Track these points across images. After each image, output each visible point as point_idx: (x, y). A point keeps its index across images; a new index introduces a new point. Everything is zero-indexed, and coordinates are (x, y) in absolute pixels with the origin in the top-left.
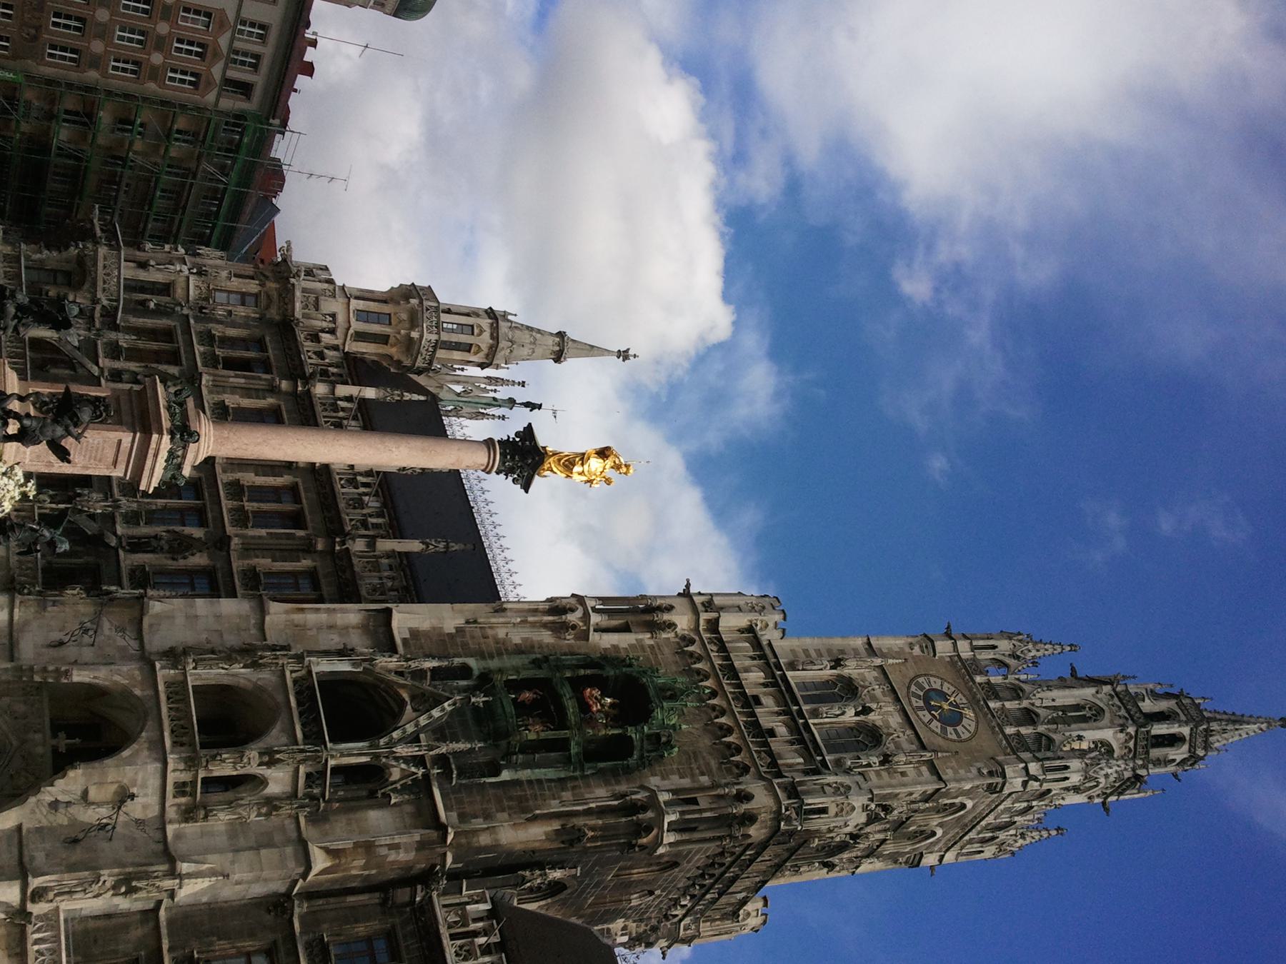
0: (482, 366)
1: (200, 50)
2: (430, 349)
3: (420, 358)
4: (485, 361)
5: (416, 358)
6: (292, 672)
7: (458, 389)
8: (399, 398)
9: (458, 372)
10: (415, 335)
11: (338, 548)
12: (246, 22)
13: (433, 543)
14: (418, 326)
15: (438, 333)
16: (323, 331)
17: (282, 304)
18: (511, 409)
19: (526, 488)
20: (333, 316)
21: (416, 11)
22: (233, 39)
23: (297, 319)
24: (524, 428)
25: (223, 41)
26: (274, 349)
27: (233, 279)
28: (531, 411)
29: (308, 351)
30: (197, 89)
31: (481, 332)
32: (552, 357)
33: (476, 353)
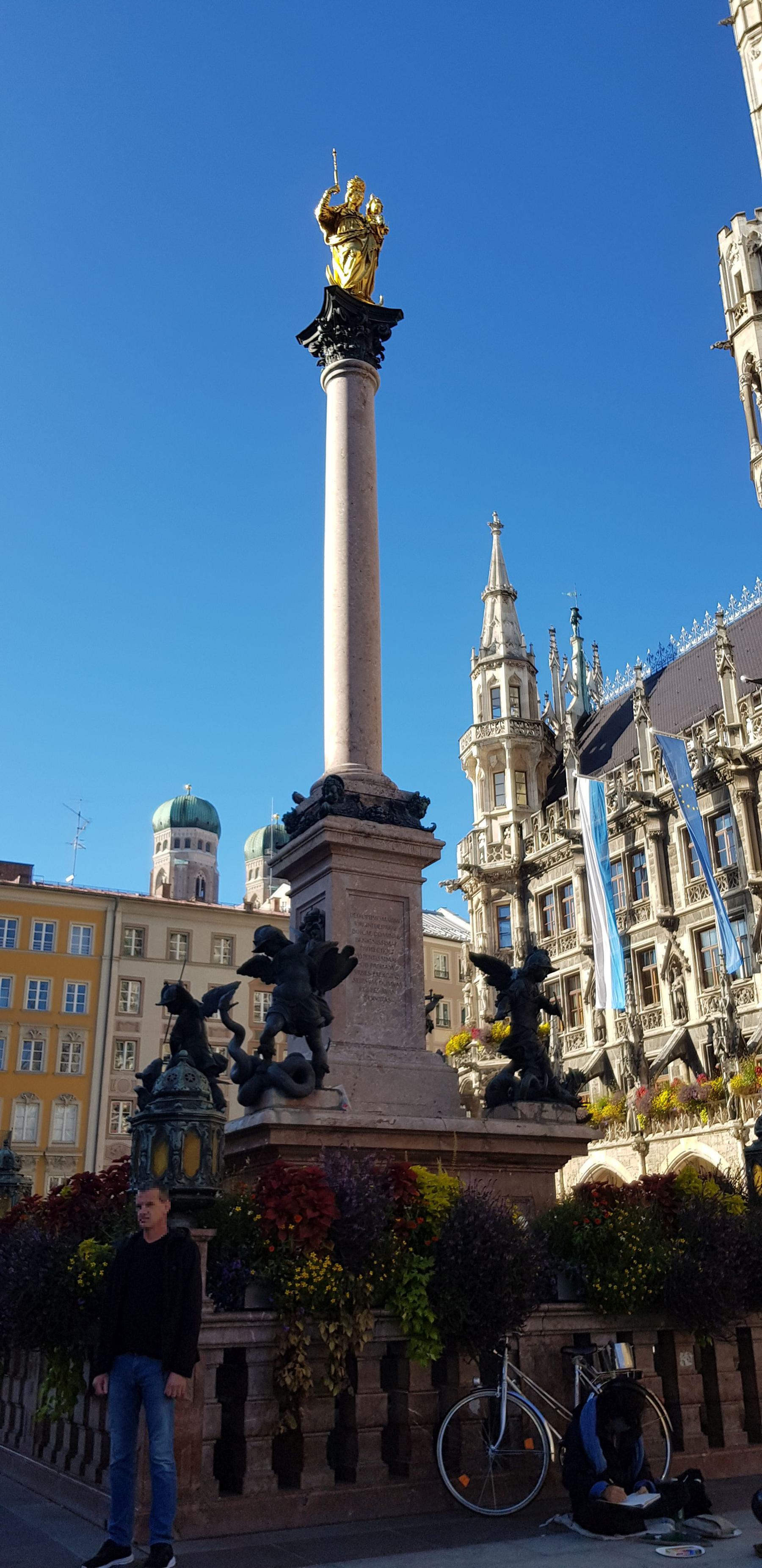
0: (534, 672)
2: (522, 725)
4: (526, 669)
11: (743, 767)
13: (721, 663)
15: (502, 720)
16: (520, 835)
18: (583, 639)
19: (394, 316)
20: (504, 828)
26: (547, 881)
27: (484, 931)
28: (581, 618)
29: (543, 846)
32: (510, 601)
33: (519, 680)
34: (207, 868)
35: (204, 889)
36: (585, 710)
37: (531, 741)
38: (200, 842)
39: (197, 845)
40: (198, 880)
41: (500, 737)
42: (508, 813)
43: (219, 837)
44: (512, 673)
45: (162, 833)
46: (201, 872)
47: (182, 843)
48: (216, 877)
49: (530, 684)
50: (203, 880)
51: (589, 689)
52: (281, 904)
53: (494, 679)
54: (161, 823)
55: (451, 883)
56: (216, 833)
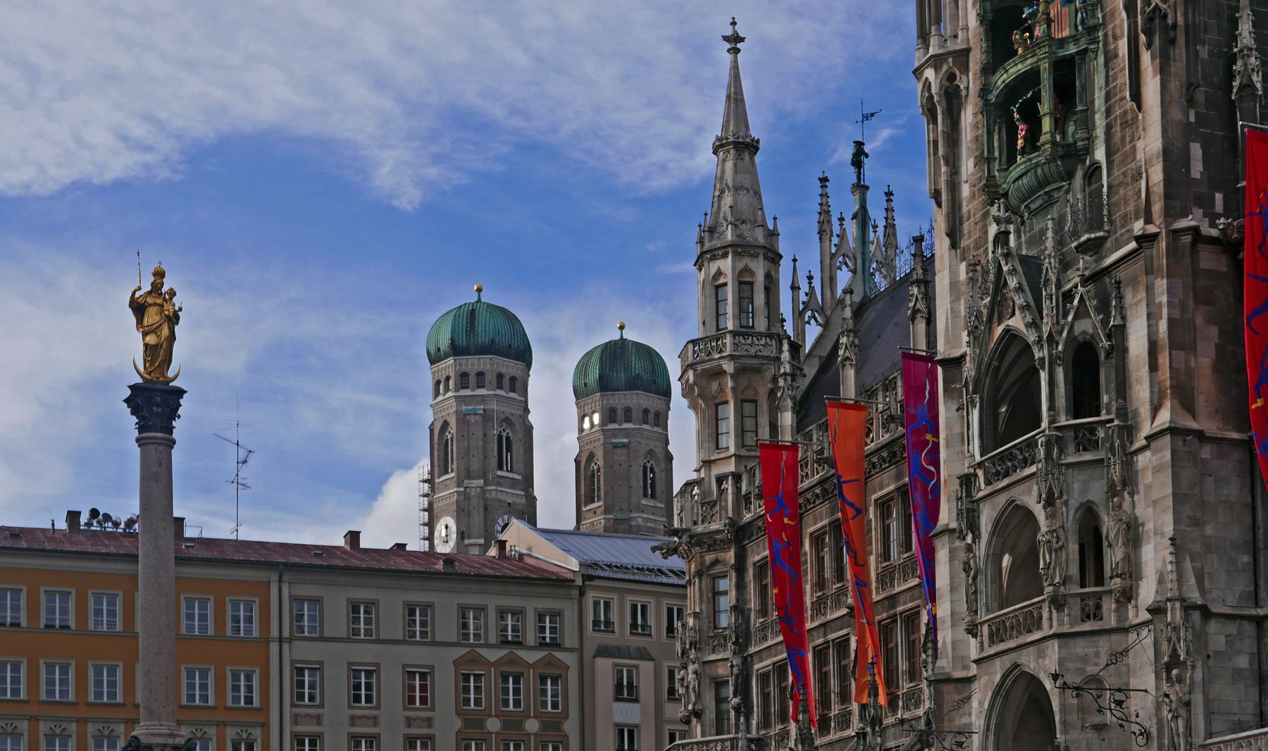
1: (511, 680)
2: (749, 341)
3: (765, 353)
4: (761, 258)
5: (764, 358)
6: (980, 490)
7: (844, 278)
8: (789, 378)
9: (817, 283)
10: (729, 367)
12: (464, 634)
14: (720, 366)
17: (717, 547)
21: (654, 369)
22: (487, 645)
23: (725, 526)
24: (128, 407)
25: (494, 655)
30: (560, 676)
31: (719, 273)
33: (752, 273)
34: (513, 418)
35: (509, 449)
36: (865, 293)
37: (760, 361)
38: (500, 376)
39: (494, 382)
40: (500, 437)
41: (720, 358)
42: (730, 457)
43: (529, 366)
44: (740, 265)
45: (442, 365)
46: (504, 424)
47: (472, 380)
48: (529, 429)
49: (768, 276)
50: (508, 438)
51: (875, 259)
52: (508, 548)
53: (719, 273)
54: (439, 349)
55: (665, 547)
56: (523, 361)
